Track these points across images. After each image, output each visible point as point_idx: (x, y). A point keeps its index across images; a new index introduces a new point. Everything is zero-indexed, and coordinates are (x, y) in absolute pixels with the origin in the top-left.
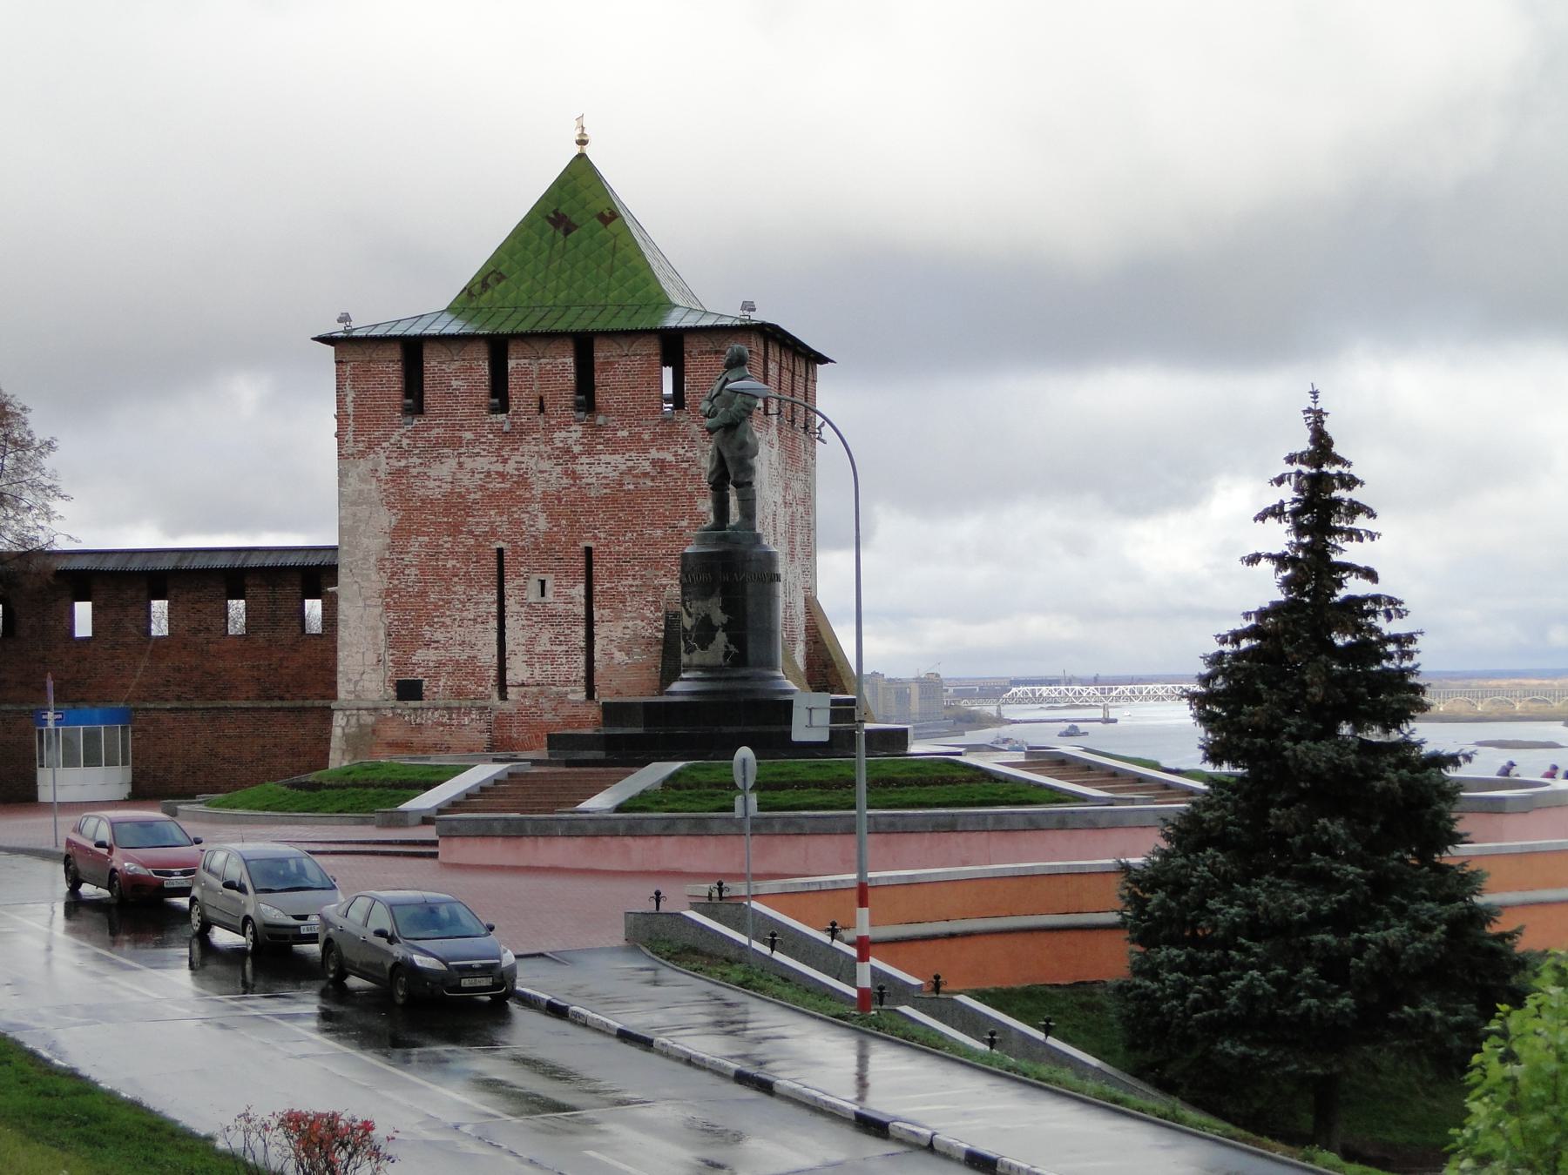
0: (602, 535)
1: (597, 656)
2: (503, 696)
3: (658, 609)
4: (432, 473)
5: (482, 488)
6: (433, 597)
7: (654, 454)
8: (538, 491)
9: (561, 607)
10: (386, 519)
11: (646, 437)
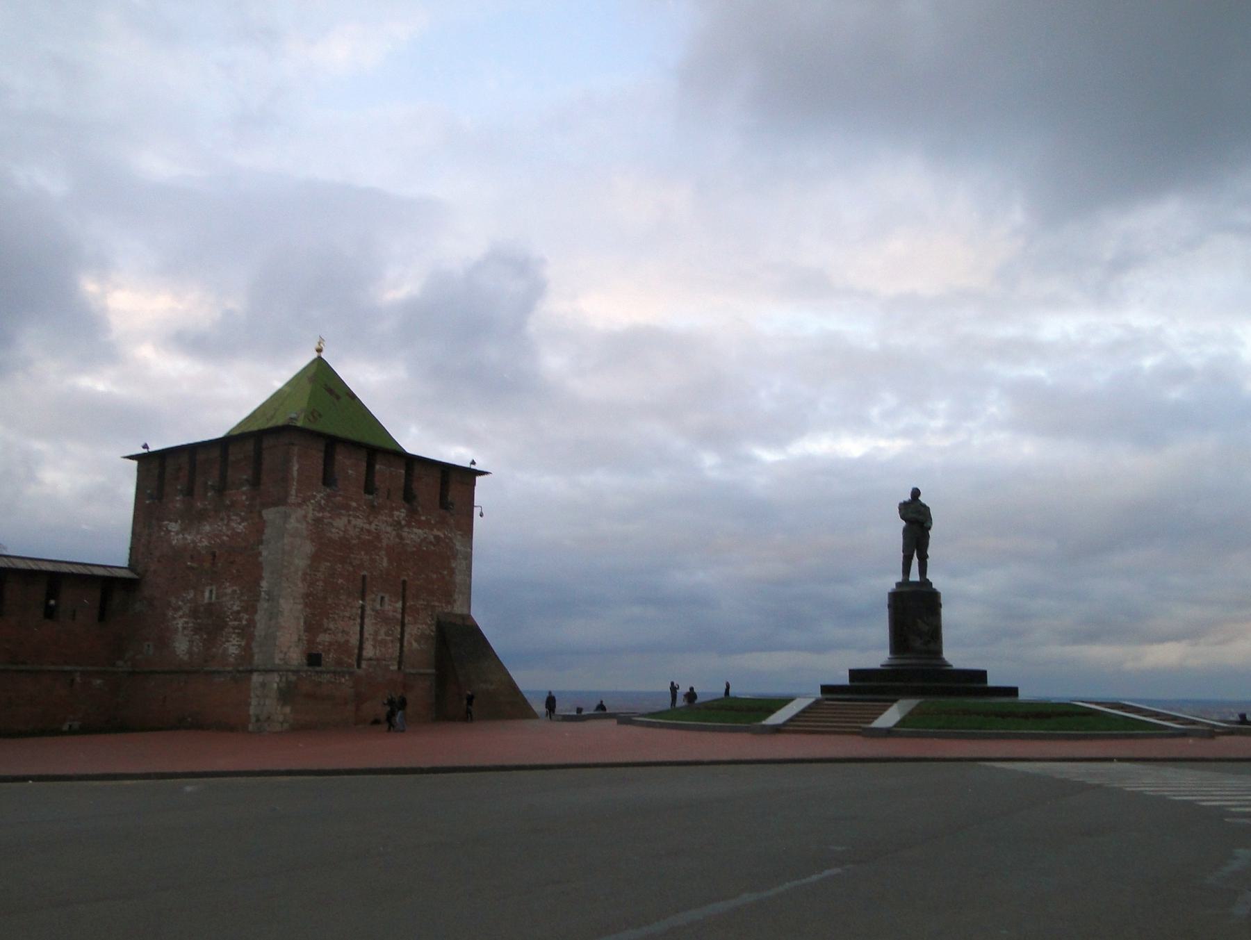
1: (405, 644)
5: (359, 537)
6: (330, 601)
7: (436, 532)
8: (385, 542)
9: (391, 614)
10: (309, 548)
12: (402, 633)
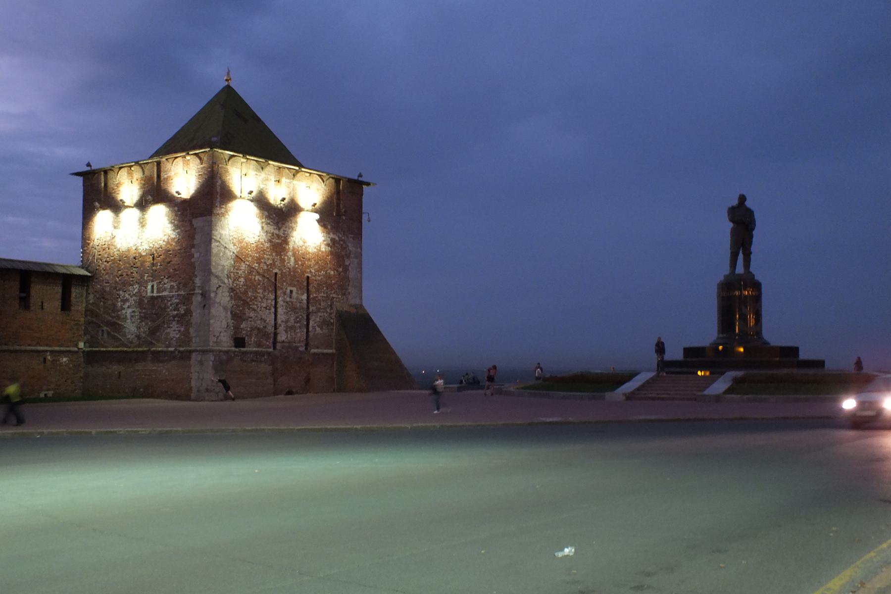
2: (275, 348)
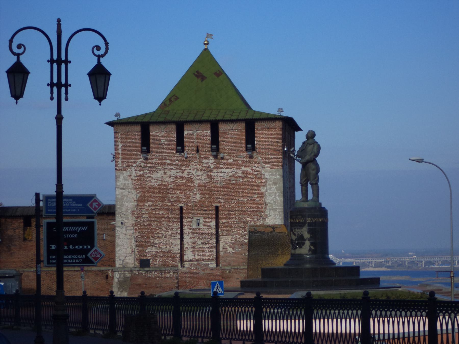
0: (222, 201)
1: (221, 249)
2: (183, 266)
3: (245, 231)
4: (154, 177)
5: (174, 182)
6: (154, 226)
7: (243, 169)
8: (196, 183)
9: (206, 230)
10: (134, 195)
11: (240, 162)
12: (217, 242)
